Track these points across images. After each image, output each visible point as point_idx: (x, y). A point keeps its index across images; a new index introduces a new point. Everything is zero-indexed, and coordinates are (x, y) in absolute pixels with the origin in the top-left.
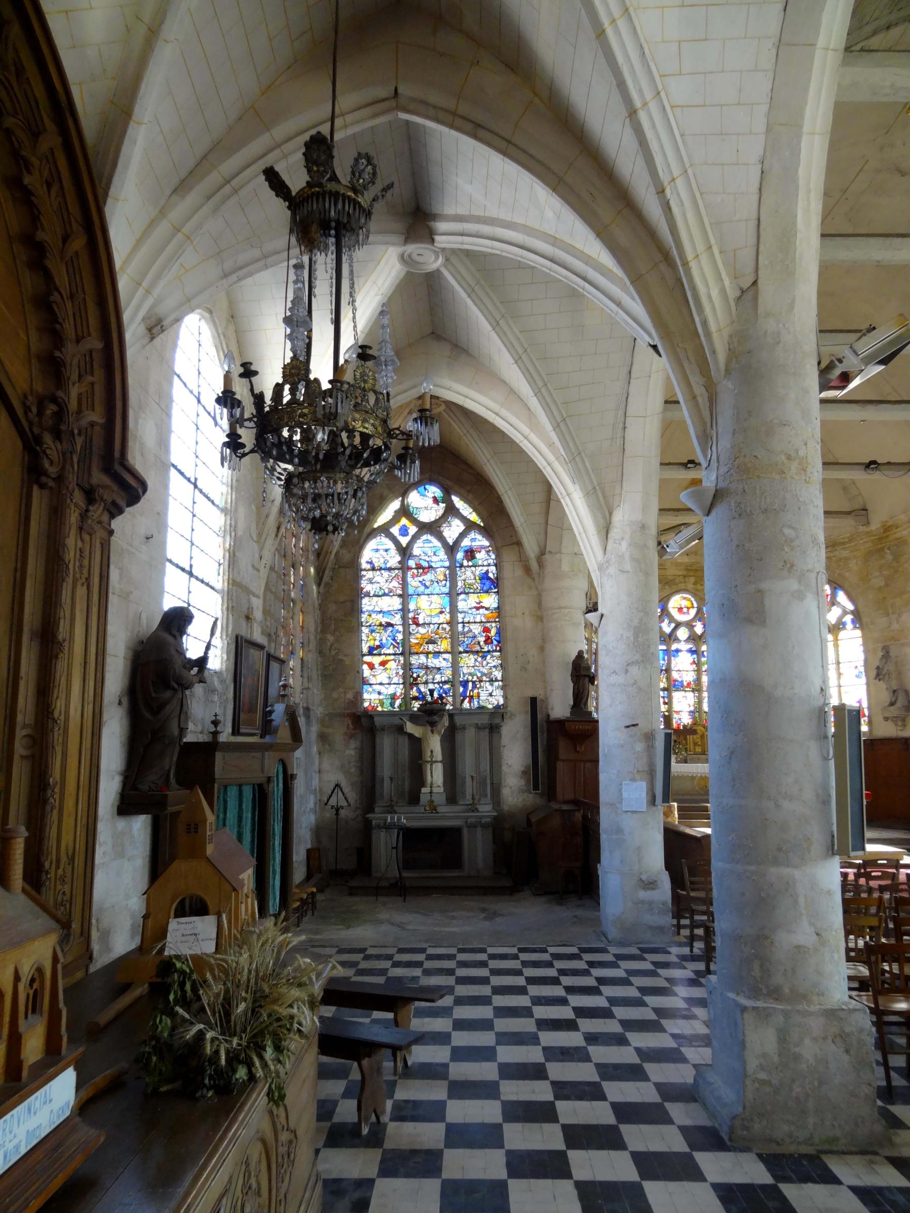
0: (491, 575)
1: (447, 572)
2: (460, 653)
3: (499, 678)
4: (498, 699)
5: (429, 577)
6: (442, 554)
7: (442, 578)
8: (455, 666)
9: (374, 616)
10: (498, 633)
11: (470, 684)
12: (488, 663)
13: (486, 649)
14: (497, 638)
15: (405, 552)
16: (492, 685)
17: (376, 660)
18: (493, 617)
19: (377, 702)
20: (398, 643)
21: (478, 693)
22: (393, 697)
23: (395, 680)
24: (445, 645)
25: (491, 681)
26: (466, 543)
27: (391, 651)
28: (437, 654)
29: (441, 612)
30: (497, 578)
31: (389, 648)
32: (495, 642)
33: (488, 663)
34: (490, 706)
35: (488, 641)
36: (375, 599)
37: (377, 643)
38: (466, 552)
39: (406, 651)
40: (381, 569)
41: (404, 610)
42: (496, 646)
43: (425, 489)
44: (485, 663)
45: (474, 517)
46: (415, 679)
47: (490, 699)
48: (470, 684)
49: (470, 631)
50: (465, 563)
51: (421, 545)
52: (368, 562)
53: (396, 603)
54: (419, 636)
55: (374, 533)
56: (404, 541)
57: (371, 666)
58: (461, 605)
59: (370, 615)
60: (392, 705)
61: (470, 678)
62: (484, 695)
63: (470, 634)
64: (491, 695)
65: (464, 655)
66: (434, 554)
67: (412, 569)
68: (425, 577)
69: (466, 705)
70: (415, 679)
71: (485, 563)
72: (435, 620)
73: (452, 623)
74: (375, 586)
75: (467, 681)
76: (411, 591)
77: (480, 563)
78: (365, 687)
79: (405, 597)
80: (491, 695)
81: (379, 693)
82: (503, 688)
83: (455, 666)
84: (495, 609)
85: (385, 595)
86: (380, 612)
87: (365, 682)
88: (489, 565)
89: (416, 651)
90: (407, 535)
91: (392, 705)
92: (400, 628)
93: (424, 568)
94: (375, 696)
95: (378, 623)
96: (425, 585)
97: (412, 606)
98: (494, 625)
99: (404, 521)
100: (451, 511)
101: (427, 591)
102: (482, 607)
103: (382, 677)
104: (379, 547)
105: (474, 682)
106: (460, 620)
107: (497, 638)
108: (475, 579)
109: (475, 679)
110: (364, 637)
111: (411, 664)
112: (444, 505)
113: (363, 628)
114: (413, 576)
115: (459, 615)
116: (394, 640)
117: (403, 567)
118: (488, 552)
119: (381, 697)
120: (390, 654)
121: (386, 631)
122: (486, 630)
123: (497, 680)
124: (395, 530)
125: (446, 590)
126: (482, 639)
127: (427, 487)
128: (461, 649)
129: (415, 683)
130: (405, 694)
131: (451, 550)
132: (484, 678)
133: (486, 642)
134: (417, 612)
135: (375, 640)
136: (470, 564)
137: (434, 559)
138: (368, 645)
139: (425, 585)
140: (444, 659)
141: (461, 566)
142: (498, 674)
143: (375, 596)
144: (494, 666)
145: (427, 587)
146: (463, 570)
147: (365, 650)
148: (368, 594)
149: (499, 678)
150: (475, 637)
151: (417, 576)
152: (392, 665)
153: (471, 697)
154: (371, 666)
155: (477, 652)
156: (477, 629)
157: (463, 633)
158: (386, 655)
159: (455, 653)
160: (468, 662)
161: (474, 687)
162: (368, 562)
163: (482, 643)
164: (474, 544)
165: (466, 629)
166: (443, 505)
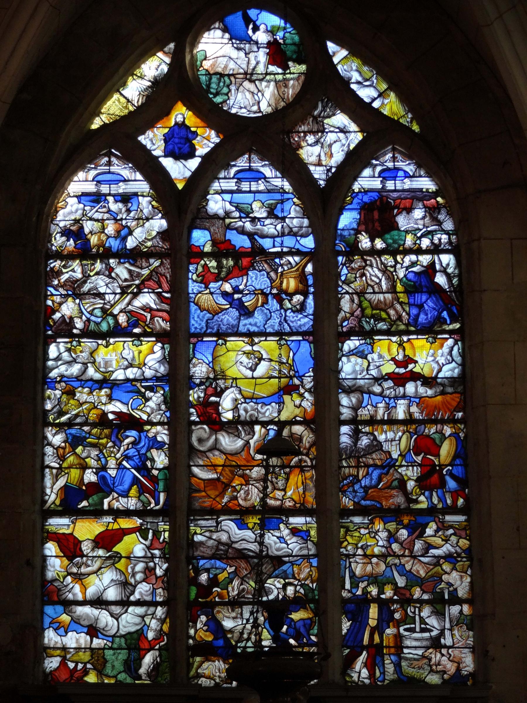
0: (440, 279)
1: (309, 268)
2: (346, 513)
4: (459, 656)
5: (257, 279)
6: (294, 216)
7: (291, 284)
8: (328, 553)
9: (82, 395)
10: (461, 454)
11: (373, 611)
12: (429, 546)
13: (423, 503)
14: (458, 471)
15: (182, 205)
16: (439, 614)
17: (86, 530)
18: (445, 405)
19: (85, 656)
20: (154, 480)
21: (399, 637)
22: (135, 643)
23: (143, 590)
24: (293, 488)
25: (439, 603)
26: (367, 180)
27: (132, 503)
28: (270, 516)
29: (289, 389)
30: (459, 290)
31: (125, 494)
32: (452, 484)
33: (429, 546)
34: (434, 679)
36: (88, 344)
37: (90, 477)
38: (366, 209)
39: (178, 502)
40: (106, 254)
41: (175, 379)
42: (455, 495)
43: (248, 20)
44: (418, 545)
45: (391, 106)
46: (205, 591)
47: (436, 657)
48: (373, 611)
50: (365, 242)
51: (232, 185)
52: (66, 233)
53: (153, 357)
54: (219, 459)
55: (88, 148)
56: (179, 171)
57: (70, 547)
58: (349, 368)
59: (70, 393)
60: (132, 666)
61: (374, 591)
62: (414, 645)
63: (376, 457)
64: (436, 644)
65: (357, 520)
66: (271, 214)
67: (201, 255)
68: (241, 283)
69: (360, 671)
70: (205, 591)
71: (425, 243)
72: (269, 412)
73: (322, 420)
74: (88, 305)
75: (365, 601)
76: (197, 321)
77: (409, 240)
78: (49, 610)
79: (178, 341)
80: (436, 644)
81: (93, 631)
82: (471, 623)
83: (328, 553)
84: (452, 380)
85: (117, 331)
86: (103, 383)
87: (52, 594)
88: (436, 250)
89: (207, 503)
90: (191, 154)
91: (132, 666)
92: (162, 435)
93: (237, 254)
94: (74, 639)
95: (93, 416)
96: (240, 306)
97: (200, 370)
98: (448, 431)
99: (181, 114)
100: (324, 90)
101: (246, 324)
102: (414, 377)
103: (104, 583)
104: (104, 189)
105: (384, 605)
106: (346, 413)
107: (458, 471)
108: (393, 290)
109: (389, 593)
110: (51, 460)
111: (193, 545)
112: (303, 68)
113: (49, 433)
114: (205, 279)
115: (345, 400)
116: (142, 468)
117: (175, 249)
118: (432, 212)
119: (97, 643)
120: (127, 513)
121: (118, 443)
122: (425, 446)
123: (455, 600)
124: (153, 140)
125: (304, 322)
126: (411, 474)
127: (252, 13)
128: (347, 502)
129: (205, 602)
130: (172, 634)
131: (321, 200)
132: (417, 593)
133: (422, 482)
134: (216, 383)
135: (84, 467)
136: (379, 244)
137: (270, 227)
138: (61, 482)
139: (240, 306)
140: (295, 532)
141: (353, 249)
142: (459, 581)
143: (86, 333)
145: (246, 312)
146: (357, 262)
147: (52, 496)
148: (65, 329)
149: (462, 593)
150: (389, 465)
151: (217, 278)
152: (135, 546)
153: (376, 653)
154: (70, 547)
155: (392, 514)
156: (394, 442)
157: (355, 454)
158: (117, 514)
159: (328, 515)
160: (369, 541)
162: (66, 233)
163: (410, 485)
164: (390, 185)
165: (364, 441)
166: (297, 69)
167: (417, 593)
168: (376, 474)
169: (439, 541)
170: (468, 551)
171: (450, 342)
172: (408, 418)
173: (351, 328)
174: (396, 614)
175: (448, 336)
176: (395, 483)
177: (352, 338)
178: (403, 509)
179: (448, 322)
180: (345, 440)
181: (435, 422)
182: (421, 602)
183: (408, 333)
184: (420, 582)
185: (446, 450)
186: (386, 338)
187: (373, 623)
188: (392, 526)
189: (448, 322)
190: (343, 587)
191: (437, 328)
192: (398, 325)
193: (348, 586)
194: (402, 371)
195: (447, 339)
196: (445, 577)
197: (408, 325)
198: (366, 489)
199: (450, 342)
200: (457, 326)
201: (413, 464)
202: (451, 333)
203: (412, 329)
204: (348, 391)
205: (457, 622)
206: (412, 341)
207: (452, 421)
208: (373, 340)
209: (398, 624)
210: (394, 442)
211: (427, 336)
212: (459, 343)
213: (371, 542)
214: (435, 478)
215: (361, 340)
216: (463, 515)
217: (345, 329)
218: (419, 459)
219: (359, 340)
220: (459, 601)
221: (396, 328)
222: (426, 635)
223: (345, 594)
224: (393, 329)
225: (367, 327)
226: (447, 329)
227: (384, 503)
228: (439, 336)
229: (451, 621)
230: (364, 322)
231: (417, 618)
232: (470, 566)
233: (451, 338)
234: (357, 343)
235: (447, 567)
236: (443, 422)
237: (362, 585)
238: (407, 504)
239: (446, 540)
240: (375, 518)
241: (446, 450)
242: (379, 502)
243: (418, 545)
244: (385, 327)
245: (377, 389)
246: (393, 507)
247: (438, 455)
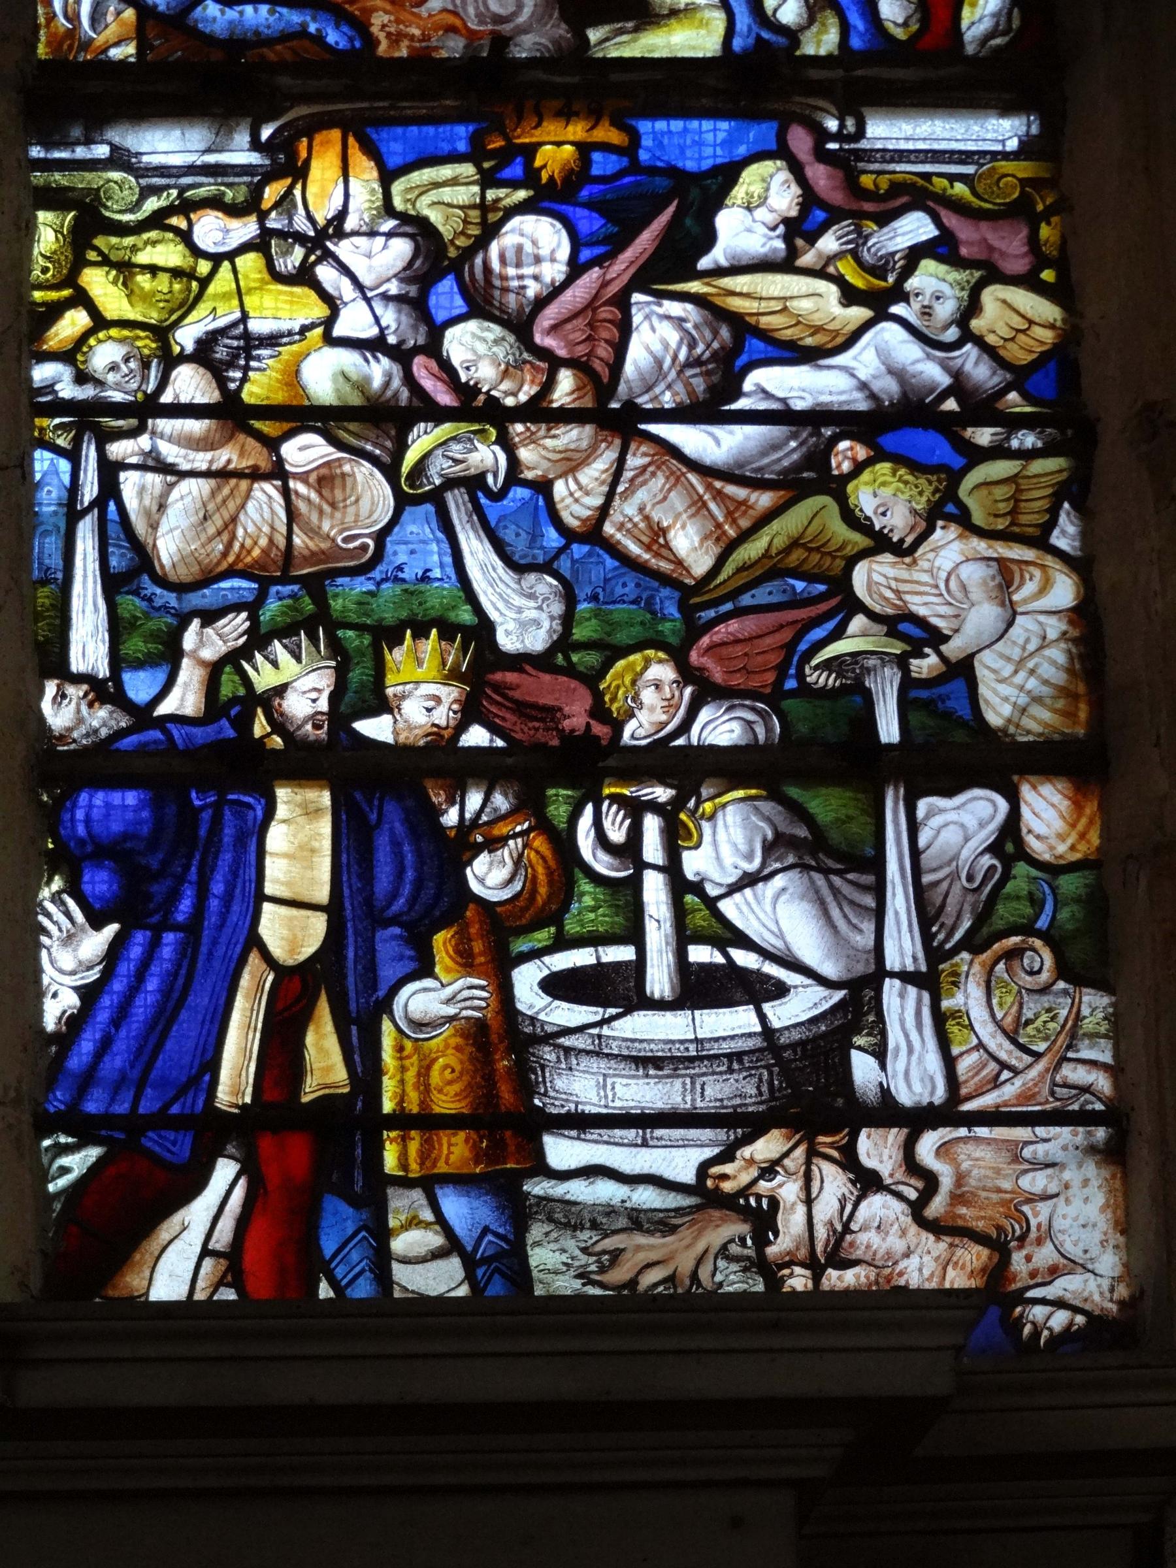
3: (1017, 685)
11: (298, 842)
12: (736, 346)
16: (837, 859)
21: (503, 1047)
25: (830, 778)
33: (736, 346)
44: (658, 335)
48: (298, 842)
61: (302, 686)
64: (809, 1092)
65: (167, 145)
75: (235, 760)
105: (376, 790)
109: (420, 700)
123: (955, 747)
132: (649, 697)
142: (995, 612)
144: (885, 424)
149: (1017, 685)
161: (401, 892)
167: (649, 697)
169: (818, 302)
170: (1056, 387)
174: (481, 864)
178: (531, 62)
182: (691, 771)
184: (679, 612)
187: (290, 935)
188: (445, 193)
190: (53, 659)
193: (88, 647)
196: (872, 578)
205: (974, 925)
209: (496, 942)
213: (278, 310)
216: (1006, 110)
220: (999, 762)
222: (733, 1023)
223: (62, 712)
227: (378, 21)
229: (927, 914)
231: (655, 889)
232: (1074, 491)
235: (885, 497)
237: (204, 643)
238: (562, 31)
239: (879, 297)
240: (311, 128)
242: (341, 16)
243: (658, 335)
246: (453, 47)
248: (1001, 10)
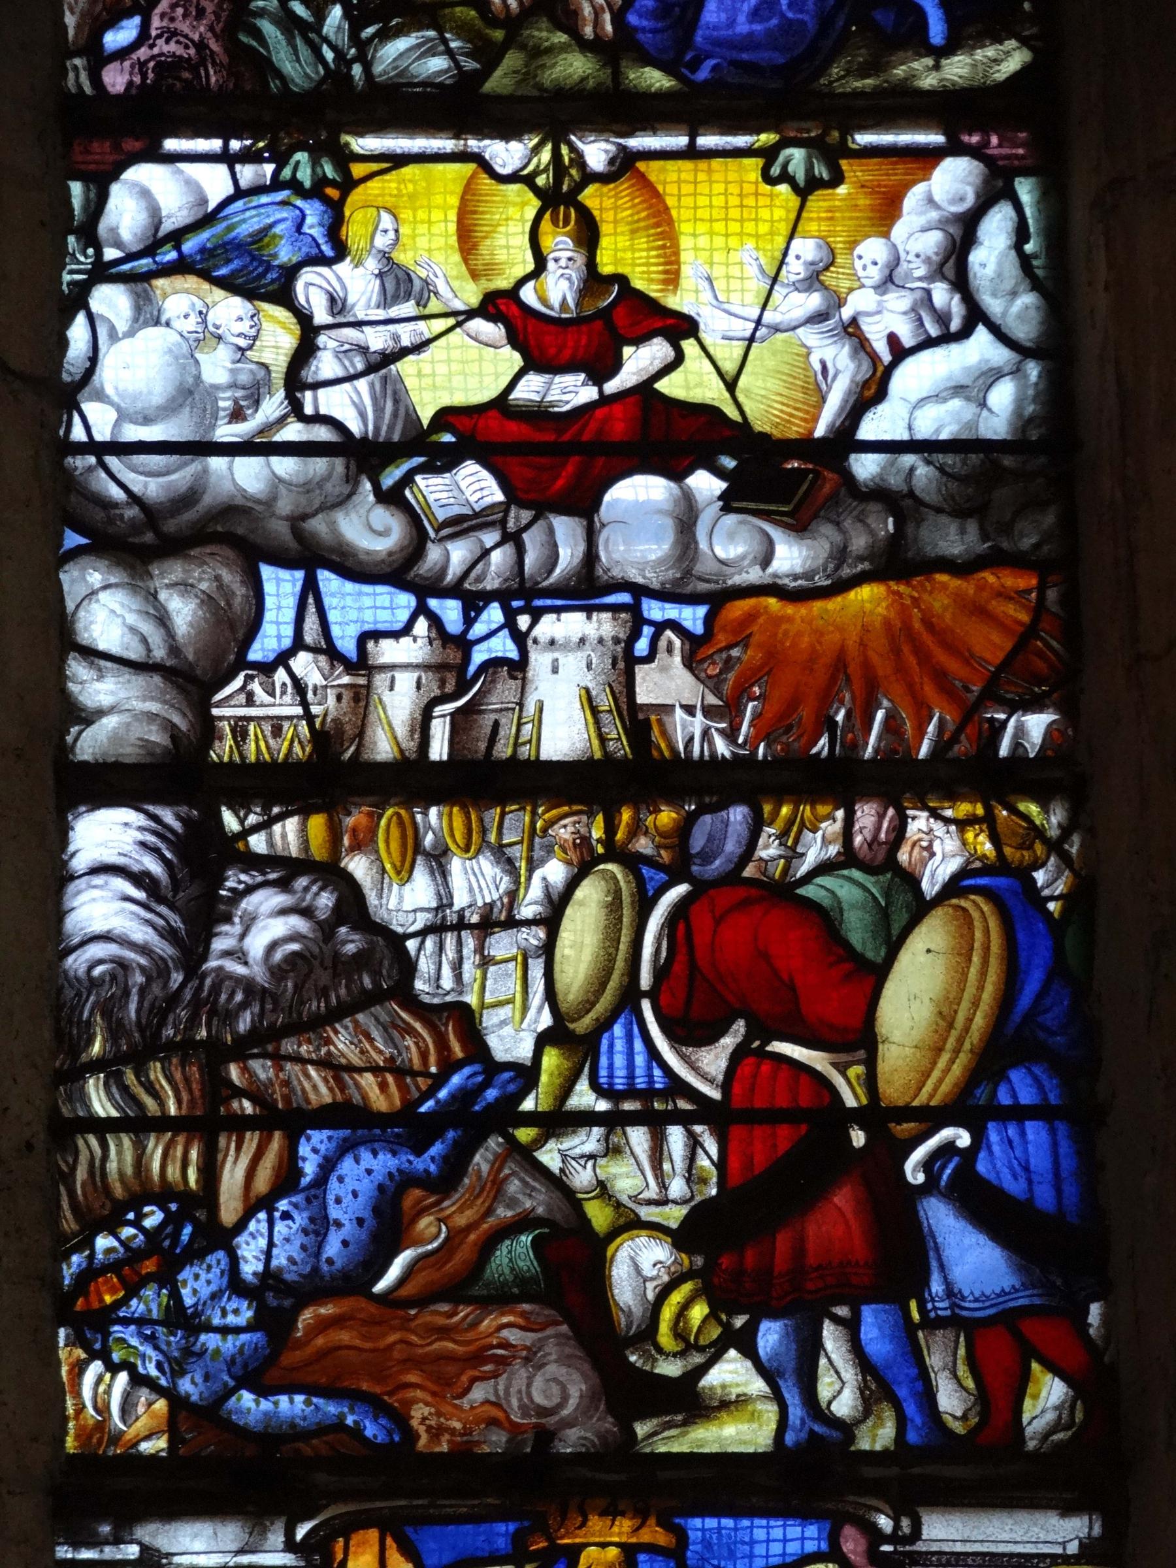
14: (1023, 1157)
32: (971, 1261)
35: (797, 1216)
42: (1001, 1346)
49: (358, 965)
98: (940, 848)
102: (670, 435)
106: (116, 711)
107: (1023, 1157)
115: (107, 614)
122: (756, 968)
128: (110, 1398)
150: (466, 1112)
156: (511, 939)
157: (179, 1018)
163: (639, 1265)
165: (264, 928)
168: (360, 1176)
171: (953, 180)
172: (621, 747)
173: (167, 67)
175: (936, 139)
176: (517, 1254)
177: (171, 144)
178: (577, 1459)
179: (937, 31)
180: (104, 915)
181: (840, 781)
183: (619, 110)
185: (920, 994)
186: (446, 144)
189: (937, 31)
191: (844, 78)
192: (537, 53)
194: (572, 391)
195: (928, 158)
197: (613, 51)
198: (275, 1298)
199: (953, 180)
200: (1009, 60)
201: (656, 1105)
202: (962, 116)
203: (655, 79)
204: (141, 543)
206: (652, 170)
207: (973, 775)
208: (344, 158)
210: (511, 939)
211: (766, 138)
212: (1025, 190)
214: (837, 1220)
215: (248, 156)
216: (1067, 1510)
217: (116, 79)
218: (708, 1067)
219: (225, 158)
221: (527, 76)
224: (499, 81)
225: (294, 66)
226: (929, 82)
227: (419, 1412)
228: (864, 139)
230: (268, 28)
233: (954, 148)
234: (215, 182)
236: (903, 782)
238: (609, 1424)
240: (347, 1527)
241: (920, 994)
242: (378, 1406)
244: (437, 64)
245: (369, 529)
246: (496, 1441)
247: (858, 1039)
248: (1063, 1403)
